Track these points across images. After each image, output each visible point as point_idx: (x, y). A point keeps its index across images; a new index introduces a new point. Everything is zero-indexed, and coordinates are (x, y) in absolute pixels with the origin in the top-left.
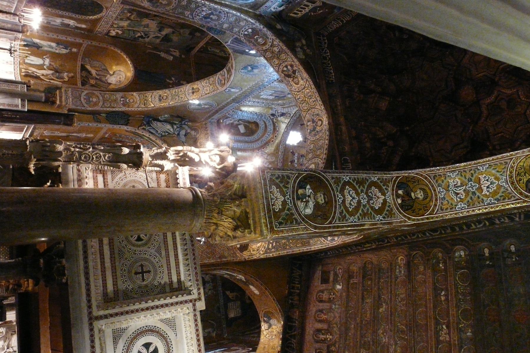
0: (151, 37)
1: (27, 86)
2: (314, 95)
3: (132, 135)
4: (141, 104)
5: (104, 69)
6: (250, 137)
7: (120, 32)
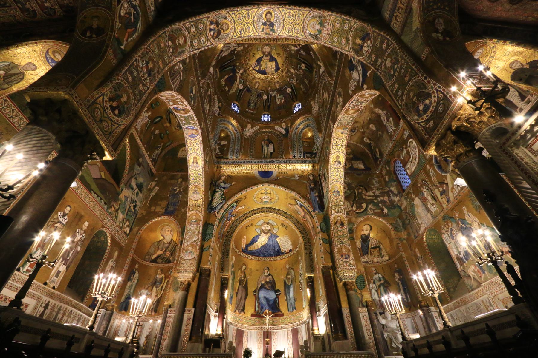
0: (136, 199)
1: (170, 307)
2: (244, 11)
3: (221, 223)
5: (158, 244)
6: (232, 138)
7: (127, 223)
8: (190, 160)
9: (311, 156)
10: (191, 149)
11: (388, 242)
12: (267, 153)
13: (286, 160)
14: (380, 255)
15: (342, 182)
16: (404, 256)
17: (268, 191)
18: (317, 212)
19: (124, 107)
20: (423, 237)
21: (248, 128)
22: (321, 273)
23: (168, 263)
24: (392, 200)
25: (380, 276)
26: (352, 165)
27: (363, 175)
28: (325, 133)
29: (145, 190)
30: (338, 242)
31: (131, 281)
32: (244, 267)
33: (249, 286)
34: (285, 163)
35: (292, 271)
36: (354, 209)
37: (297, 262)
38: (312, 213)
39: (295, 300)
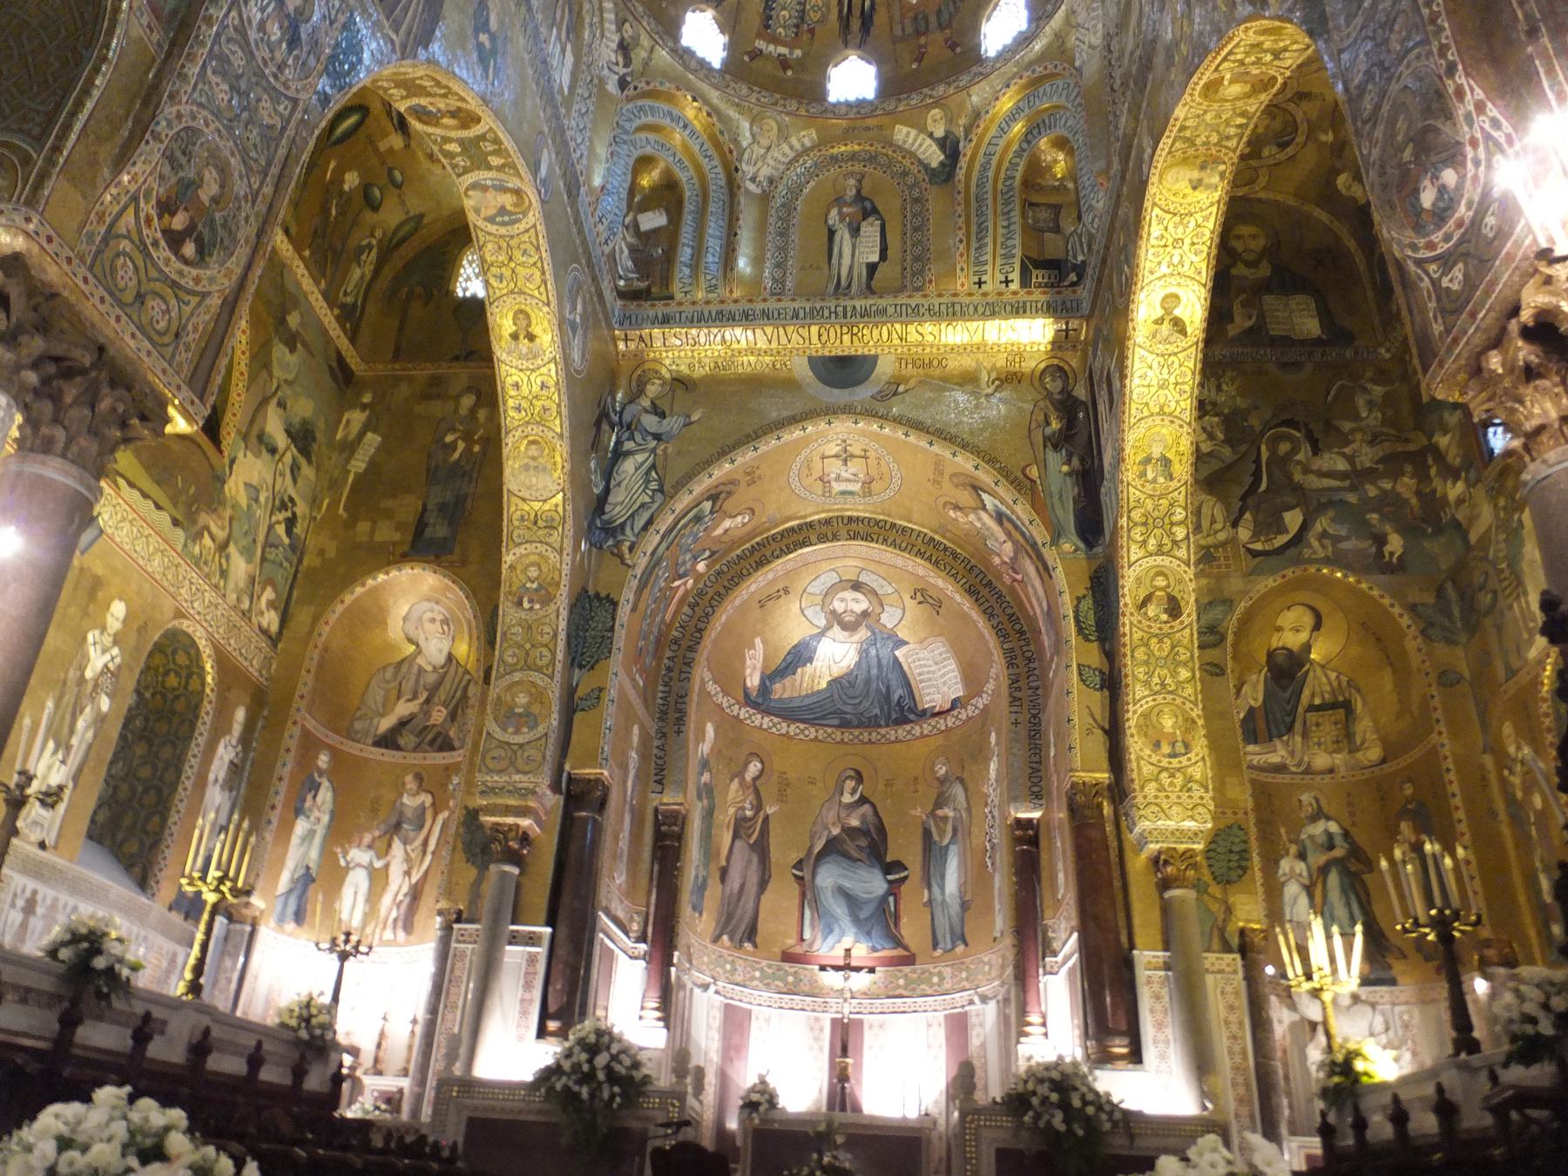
0: (292, 492)
1: (458, 920)
3: (646, 591)
4: (550, 540)
6: (687, 194)
7: (269, 594)
8: (503, 323)
9: (1061, 279)
10: (501, 278)
11: (1389, 686)
12: (851, 268)
13: (936, 301)
15: (1187, 416)
16: (1446, 751)
17: (855, 449)
18: (1067, 547)
19: (211, 223)
20: (1538, 676)
21: (765, 142)
22: (1065, 807)
23: (441, 749)
24: (1434, 491)
25: (1333, 827)
26: (1262, 316)
27: (1309, 368)
28: (1123, 178)
29: (324, 449)
30: (1147, 684)
32: (754, 768)
34: (936, 315)
35: (958, 790)
36: (1244, 534)
37: (979, 754)
38: (1043, 551)
39: (965, 906)
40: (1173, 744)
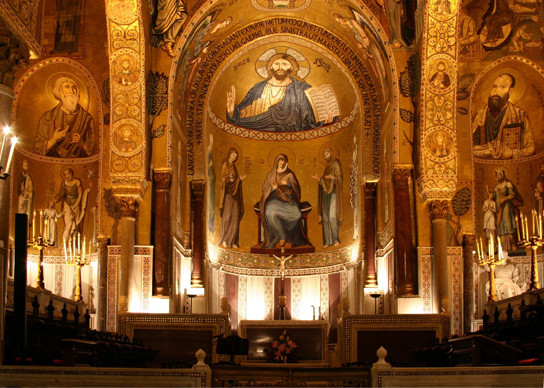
14: (520, 142)
30: (432, 120)
31: (23, 195)
32: (233, 156)
33: (244, 194)
37: (349, 147)
40: (442, 151)
